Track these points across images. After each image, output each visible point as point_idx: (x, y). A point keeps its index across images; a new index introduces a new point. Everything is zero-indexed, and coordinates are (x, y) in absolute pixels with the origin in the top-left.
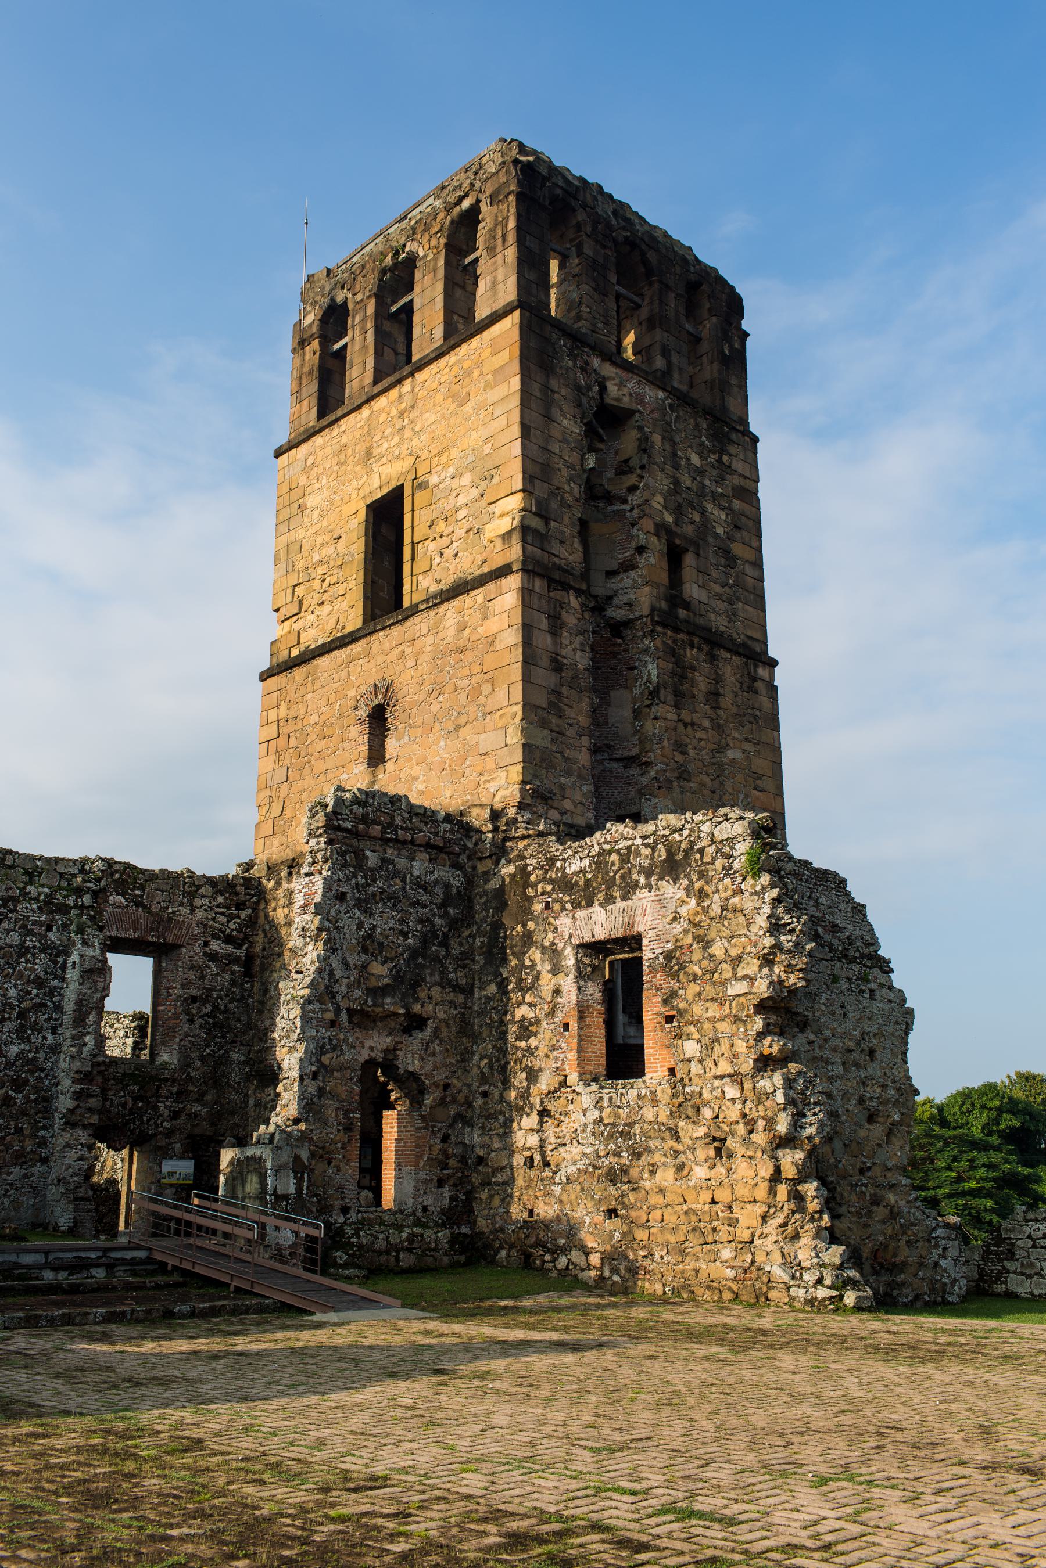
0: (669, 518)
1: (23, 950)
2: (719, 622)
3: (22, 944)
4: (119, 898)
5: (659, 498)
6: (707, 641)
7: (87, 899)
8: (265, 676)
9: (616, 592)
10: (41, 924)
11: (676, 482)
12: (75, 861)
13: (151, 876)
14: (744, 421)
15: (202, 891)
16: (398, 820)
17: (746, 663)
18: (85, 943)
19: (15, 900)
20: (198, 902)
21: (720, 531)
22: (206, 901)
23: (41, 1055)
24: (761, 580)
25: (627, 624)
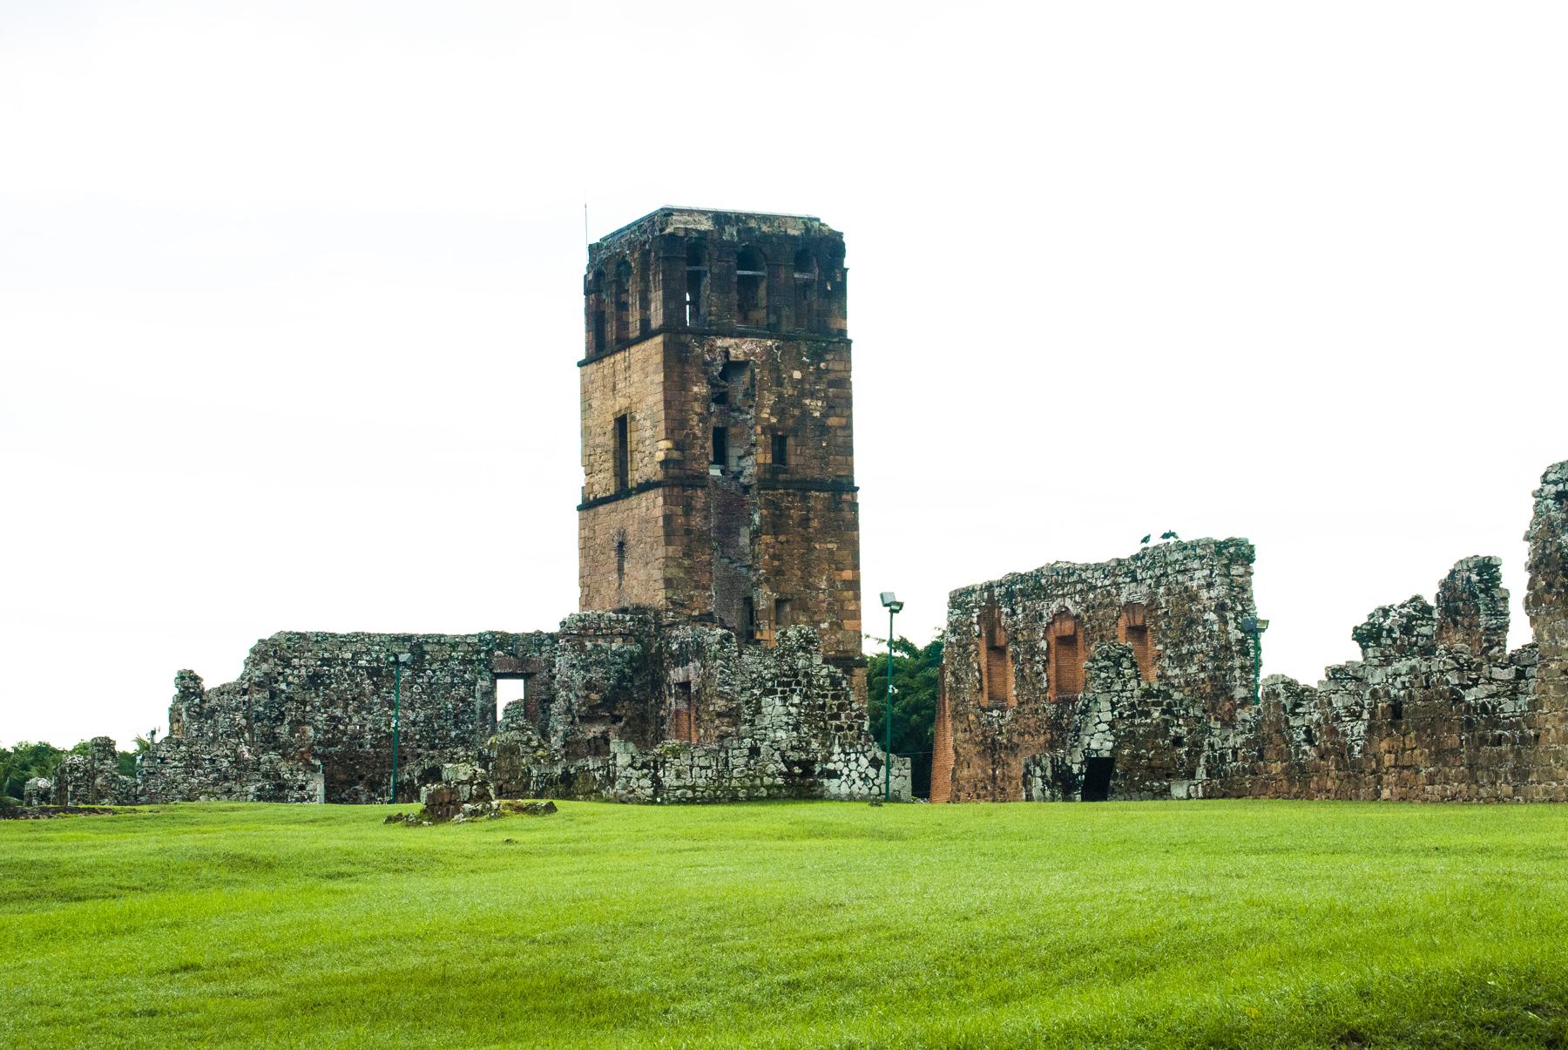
0: (774, 420)
1: (453, 685)
2: (816, 474)
3: (453, 681)
4: (500, 653)
5: (769, 411)
6: (799, 489)
7: (482, 655)
8: (580, 508)
9: (744, 468)
10: (460, 671)
11: (780, 396)
12: (475, 636)
13: (516, 637)
14: (842, 332)
15: (546, 642)
16: (602, 625)
17: (833, 495)
18: (482, 679)
19: (447, 661)
20: (543, 649)
21: (817, 414)
22: (548, 648)
23: (467, 735)
24: (851, 436)
25: (750, 486)
